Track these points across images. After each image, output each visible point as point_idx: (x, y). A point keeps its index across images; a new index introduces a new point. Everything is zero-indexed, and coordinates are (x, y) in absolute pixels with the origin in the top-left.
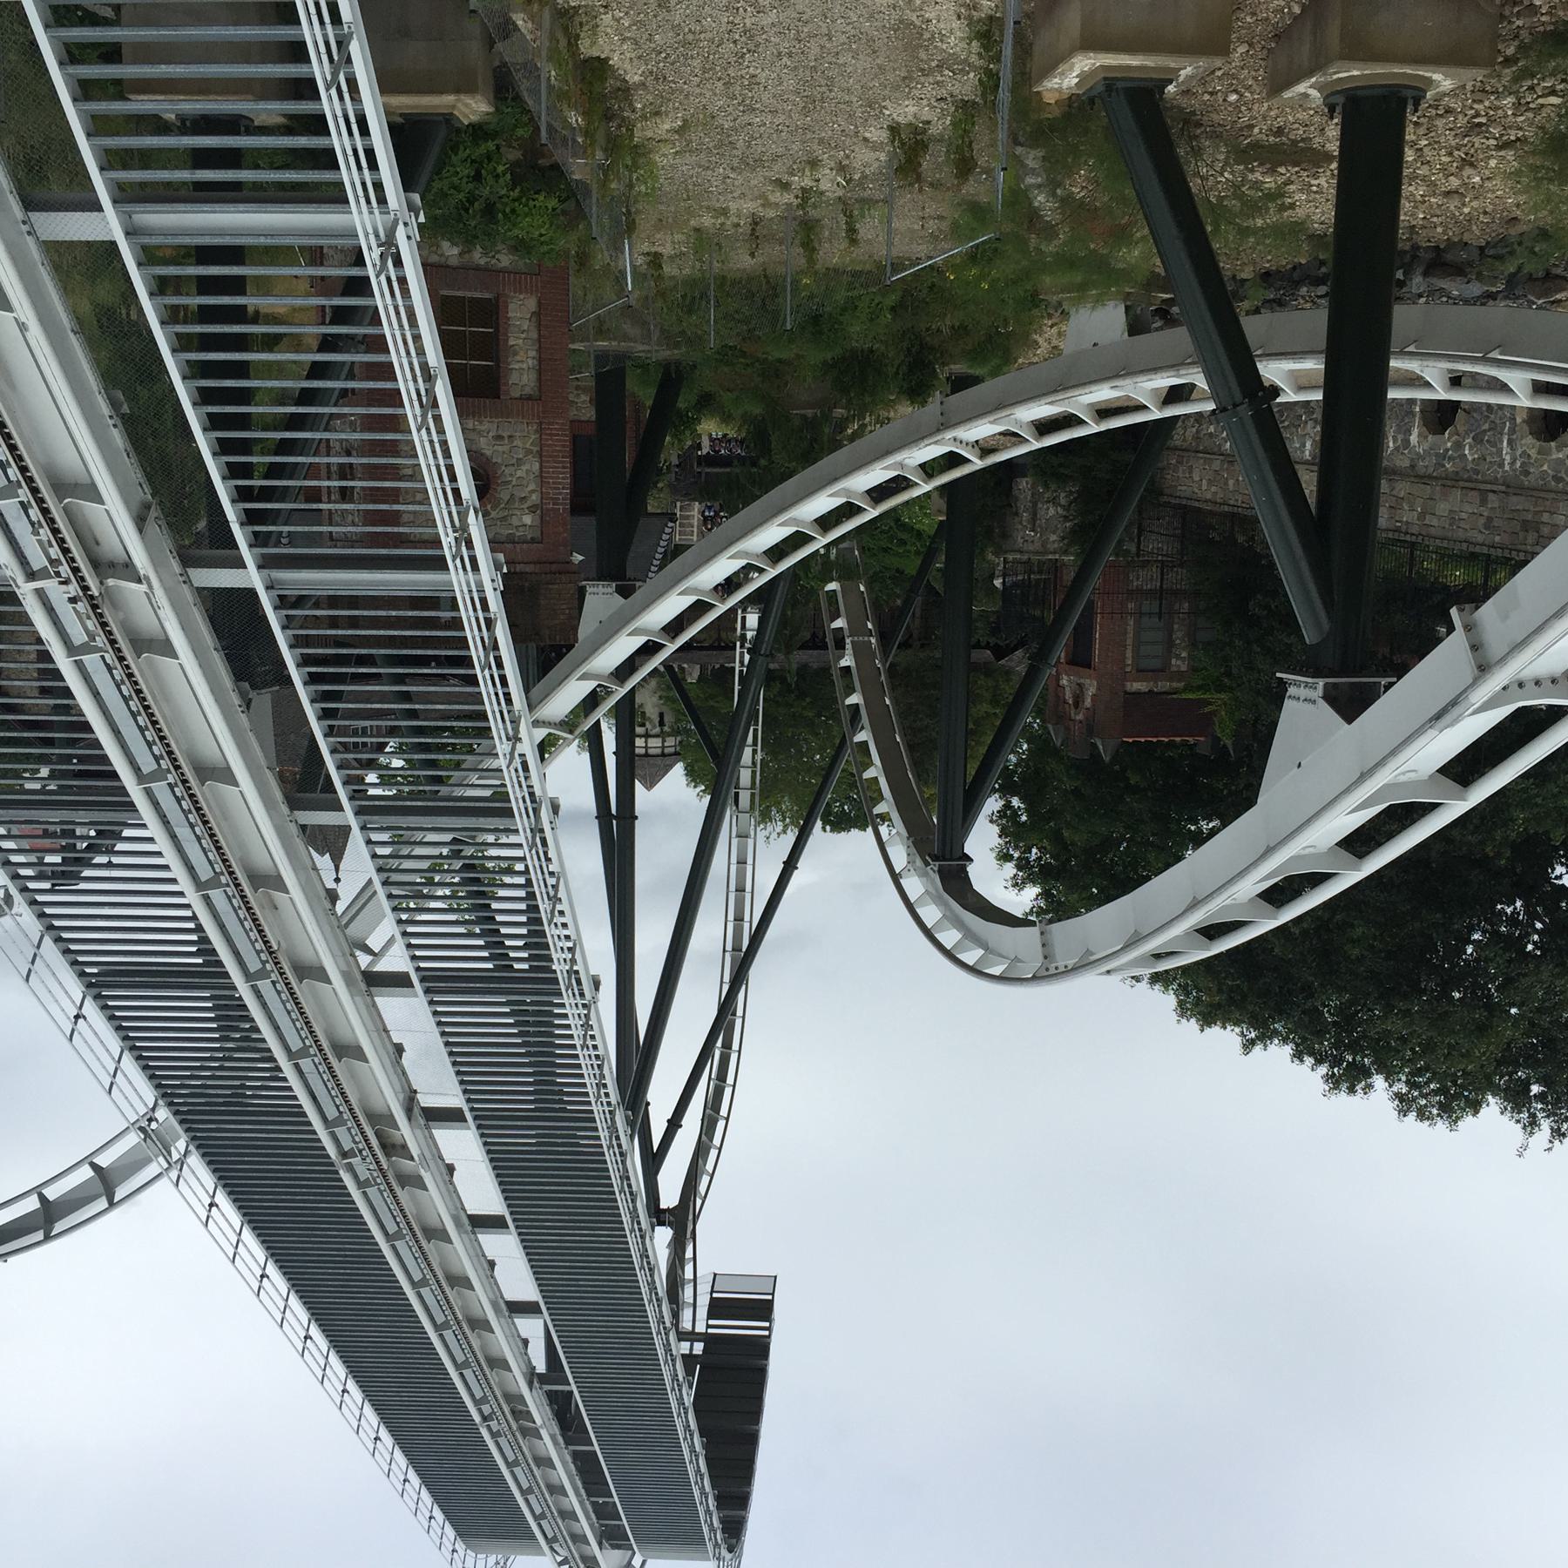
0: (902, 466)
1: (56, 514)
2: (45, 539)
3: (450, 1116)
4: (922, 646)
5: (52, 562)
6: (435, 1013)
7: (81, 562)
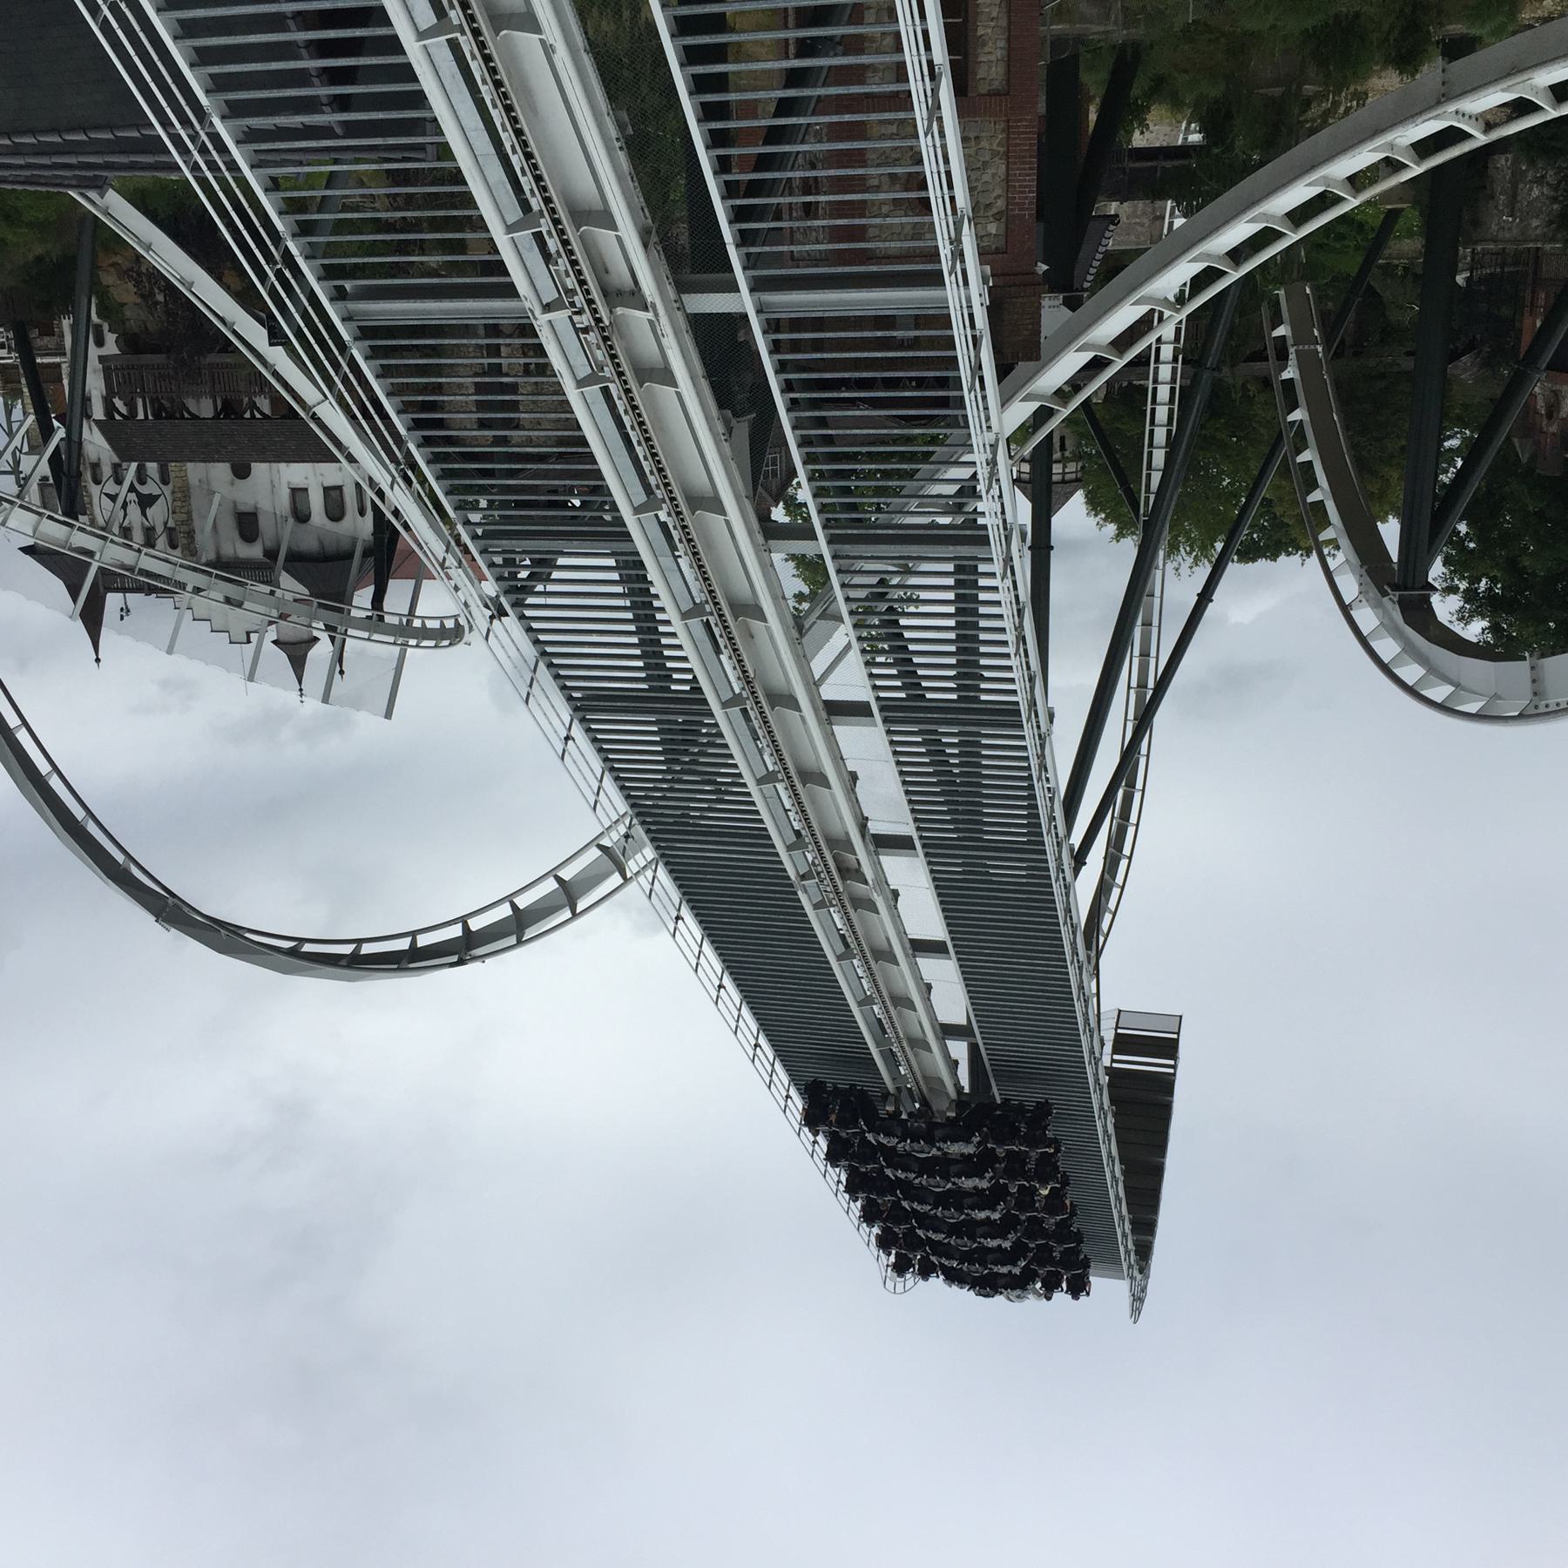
0: (1392, 146)
1: (576, 246)
2: (562, 268)
3: (899, 844)
4: (1355, 354)
5: (570, 292)
6: (892, 743)
7: (596, 295)
